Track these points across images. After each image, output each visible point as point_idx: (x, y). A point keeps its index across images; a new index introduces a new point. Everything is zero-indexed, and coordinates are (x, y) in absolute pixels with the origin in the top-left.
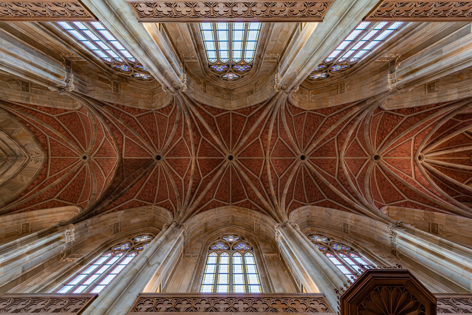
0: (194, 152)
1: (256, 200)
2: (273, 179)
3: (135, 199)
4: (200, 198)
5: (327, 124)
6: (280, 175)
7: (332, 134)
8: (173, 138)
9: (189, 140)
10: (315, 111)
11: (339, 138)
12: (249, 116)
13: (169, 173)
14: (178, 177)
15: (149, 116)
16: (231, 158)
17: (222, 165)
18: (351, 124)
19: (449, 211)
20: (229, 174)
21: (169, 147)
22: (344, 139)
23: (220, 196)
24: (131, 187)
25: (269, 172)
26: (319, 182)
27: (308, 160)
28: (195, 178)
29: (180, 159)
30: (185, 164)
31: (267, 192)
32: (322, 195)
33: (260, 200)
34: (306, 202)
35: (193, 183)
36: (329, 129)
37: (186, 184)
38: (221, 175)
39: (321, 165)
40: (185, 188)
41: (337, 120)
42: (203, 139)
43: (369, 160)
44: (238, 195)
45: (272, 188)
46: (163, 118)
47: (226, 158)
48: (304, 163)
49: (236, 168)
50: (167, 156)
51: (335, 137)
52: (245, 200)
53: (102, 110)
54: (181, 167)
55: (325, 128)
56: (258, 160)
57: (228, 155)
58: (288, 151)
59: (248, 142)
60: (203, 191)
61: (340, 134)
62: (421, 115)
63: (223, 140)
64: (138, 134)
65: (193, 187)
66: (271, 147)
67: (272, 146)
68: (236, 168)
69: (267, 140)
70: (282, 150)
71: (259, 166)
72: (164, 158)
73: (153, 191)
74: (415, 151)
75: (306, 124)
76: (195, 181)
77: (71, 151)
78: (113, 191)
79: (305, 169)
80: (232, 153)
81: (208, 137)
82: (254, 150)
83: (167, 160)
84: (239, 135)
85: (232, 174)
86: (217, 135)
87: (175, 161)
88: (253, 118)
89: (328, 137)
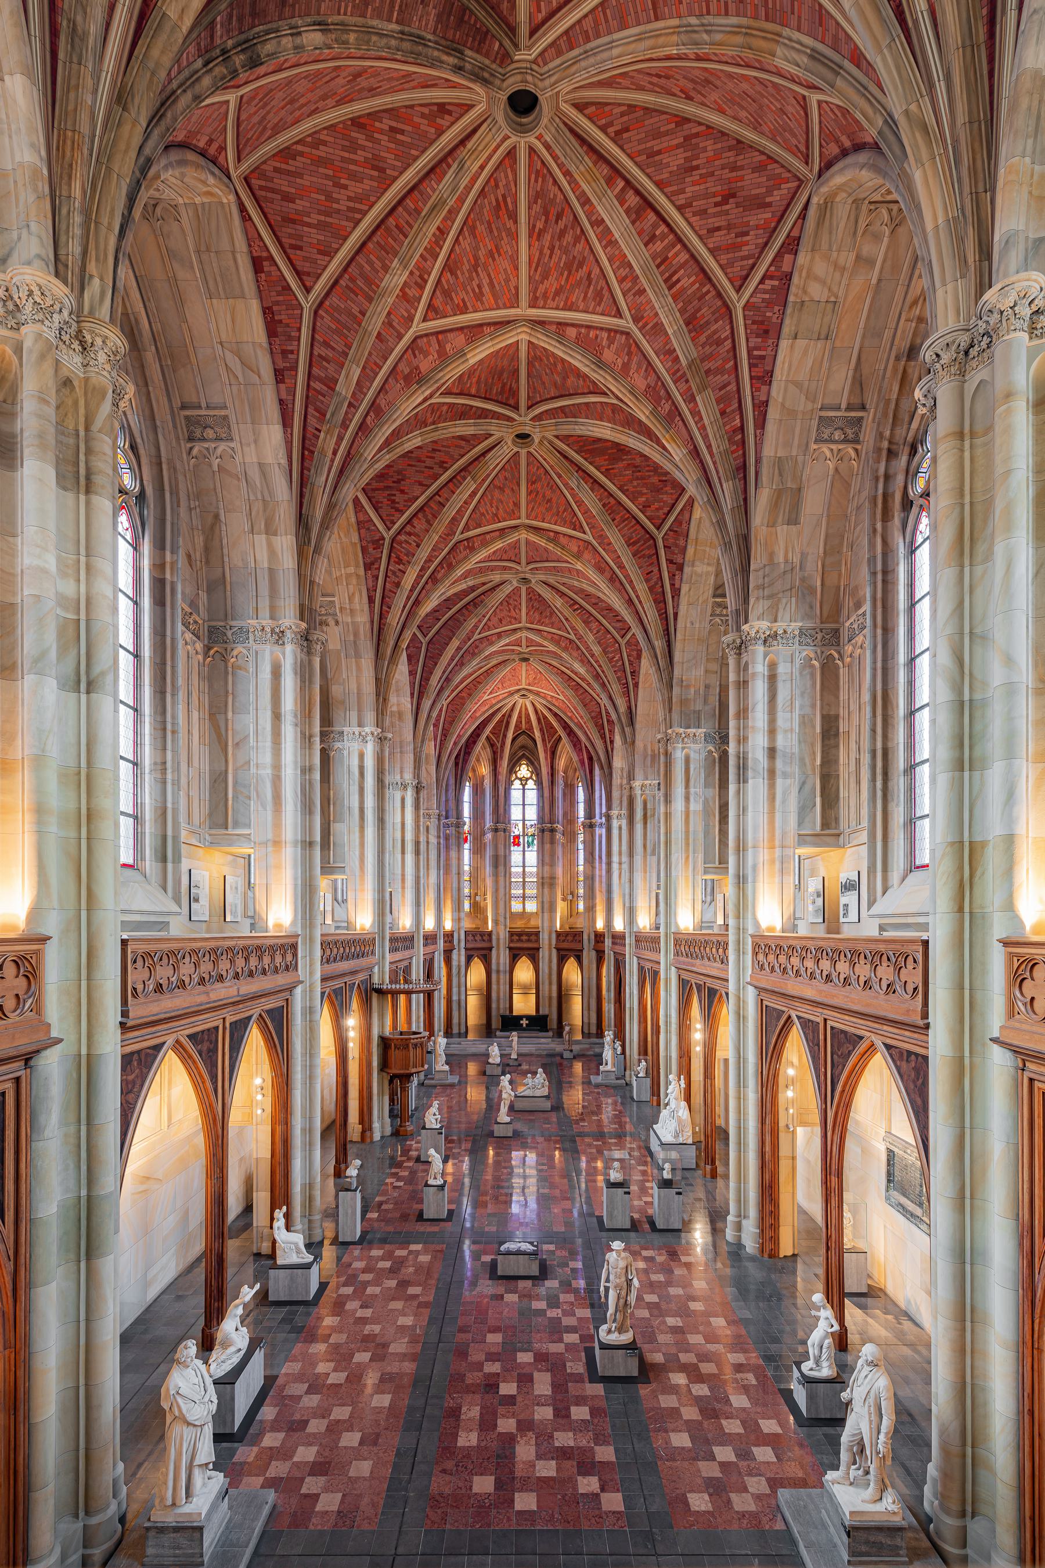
1: (394, 573)
12: (660, 543)
21: (585, 201)
26: (463, 615)
29: (515, 236)
33: (398, 585)
44: (388, 488)
49: (484, 454)
52: (380, 526)
56: (517, 505)
68: (484, 454)
71: (496, 515)
74: (538, 694)
82: (550, 501)
84: (607, 473)
87: (505, 208)
88: (650, 556)
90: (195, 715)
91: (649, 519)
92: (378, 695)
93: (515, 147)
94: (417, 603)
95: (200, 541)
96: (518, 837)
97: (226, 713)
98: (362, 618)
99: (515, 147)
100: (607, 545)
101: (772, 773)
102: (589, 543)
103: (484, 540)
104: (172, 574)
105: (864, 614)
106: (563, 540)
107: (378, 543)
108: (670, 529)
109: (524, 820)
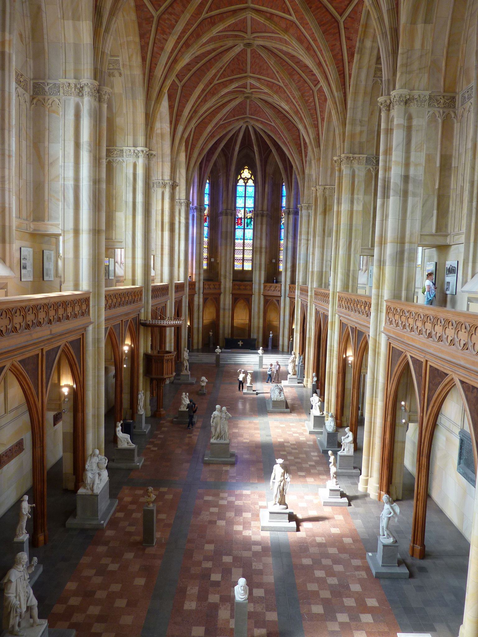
1: (160, 41)
11: (280, 88)
18: (297, 112)
19: (189, 163)
31: (179, 51)
32: (185, 76)
33: (162, 49)
41: (307, 102)
55: (299, 82)
61: (285, 92)
62: (299, 141)
90: (24, 143)
91: (336, 8)
92: (147, 125)
94: (175, 61)
95: (28, 23)
96: (241, 219)
97: (44, 142)
98: (137, 72)
100: (305, 25)
101: (405, 194)
102: (294, 23)
103: (222, 17)
104: (9, 48)
105: (472, 88)
106: (275, 19)
107: (149, 20)
108: (349, 16)
109: (245, 208)
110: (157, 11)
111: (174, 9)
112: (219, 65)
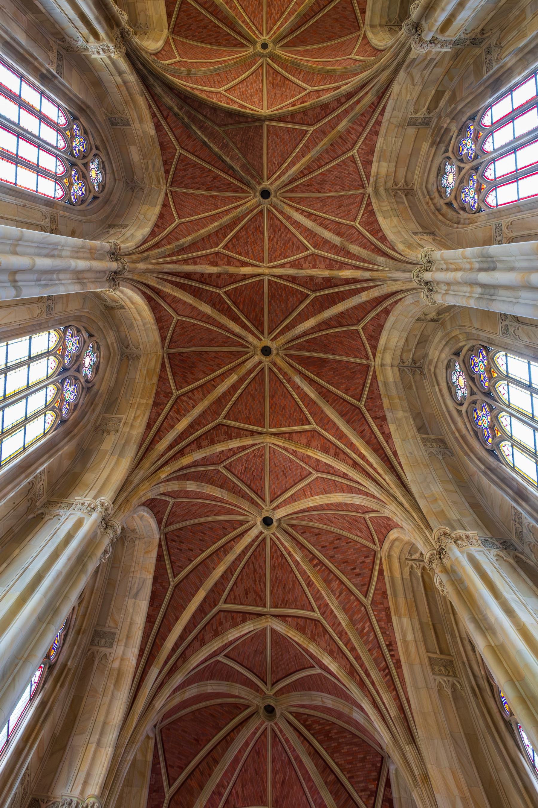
0: (279, 274)
2: (218, 454)
3: (179, 150)
4: (179, 294)
5: (349, 600)
6: (228, 468)
7: (325, 609)
8: (309, 230)
9: (305, 266)
10: (381, 572)
13: (233, 218)
14: (225, 237)
15: (355, 180)
16: (266, 351)
17: (251, 332)
20: (231, 346)
22: (312, 638)
23: (183, 328)
24: (204, 143)
25: (234, 444)
27: (261, 533)
28: (222, 277)
30: (252, 251)
34: (166, 526)
35: (211, 275)
36: (336, 602)
37: (210, 257)
38: (228, 330)
39: (251, 566)
40: (200, 257)
42: (308, 296)
43: (264, 688)
45: (198, 456)
46: (354, 211)
47: (267, 342)
48: (255, 525)
50: (269, 211)
51: (317, 615)
53: (366, 93)
54: (247, 243)
57: (274, 346)
58: (284, 489)
59: (304, 397)
60: (194, 296)
63: (307, 338)
64: (315, 157)
65: (202, 274)
66: (291, 451)
67: (295, 453)
69: (308, 445)
70: (284, 474)
72: (266, 204)
73: (196, 183)
75: (348, 541)
76: (214, 277)
77: (279, 19)
78: (196, 110)
79: (242, 523)
80: (277, 354)
81: (313, 306)
83: (261, 212)
85: (231, 353)
86: (319, 327)
89: (318, 597)
91: (352, 396)
93: (263, 210)
99: (263, 210)
106: (295, 437)
110: (178, 390)
111: (194, 395)
112: (230, 558)
